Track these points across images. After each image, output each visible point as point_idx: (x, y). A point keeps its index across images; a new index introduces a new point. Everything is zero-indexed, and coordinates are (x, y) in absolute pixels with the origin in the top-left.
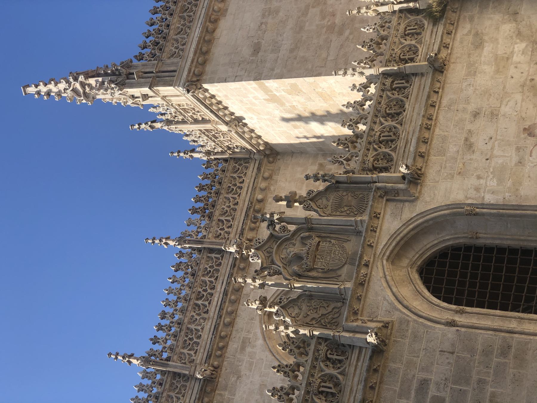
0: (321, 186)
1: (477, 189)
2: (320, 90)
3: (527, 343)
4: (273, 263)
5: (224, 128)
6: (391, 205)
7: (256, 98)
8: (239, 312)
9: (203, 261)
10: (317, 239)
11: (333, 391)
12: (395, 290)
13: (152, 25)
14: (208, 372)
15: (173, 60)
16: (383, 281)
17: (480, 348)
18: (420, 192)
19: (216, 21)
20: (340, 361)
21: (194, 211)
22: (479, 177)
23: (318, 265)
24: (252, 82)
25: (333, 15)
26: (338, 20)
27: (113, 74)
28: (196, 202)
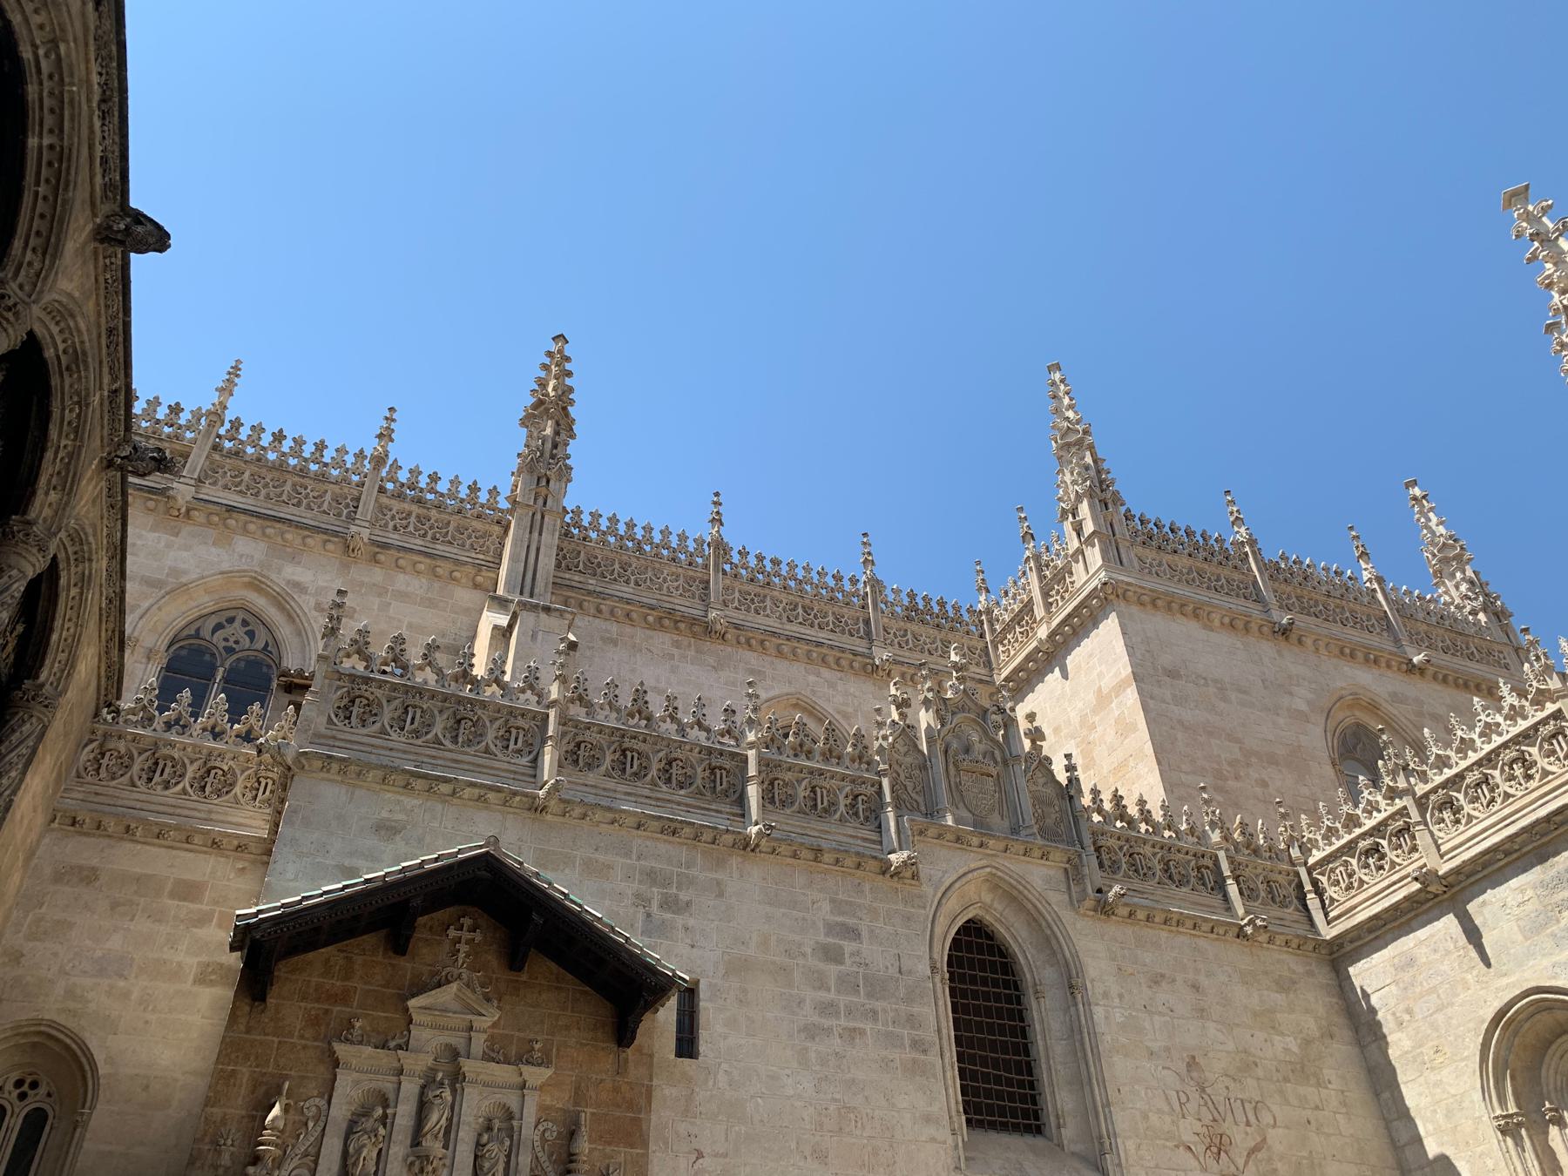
0: (1062, 777)
1: (1106, 995)
2: (1131, 764)
3: (934, 1076)
4: (953, 713)
5: (1043, 632)
6: (1061, 875)
7: (1101, 675)
8: (796, 664)
9: (852, 613)
10: (995, 773)
12: (957, 885)
13: (1172, 531)
14: (718, 627)
15: (1135, 560)
16: (965, 869)
17: (916, 1010)
18: (1085, 915)
19: (1196, 616)
20: (856, 814)
21: (912, 595)
22: (1121, 996)
23: (964, 778)
24: (1129, 670)
25: (1237, 778)
26: (1231, 784)
27: (1101, 482)
28: (924, 598)
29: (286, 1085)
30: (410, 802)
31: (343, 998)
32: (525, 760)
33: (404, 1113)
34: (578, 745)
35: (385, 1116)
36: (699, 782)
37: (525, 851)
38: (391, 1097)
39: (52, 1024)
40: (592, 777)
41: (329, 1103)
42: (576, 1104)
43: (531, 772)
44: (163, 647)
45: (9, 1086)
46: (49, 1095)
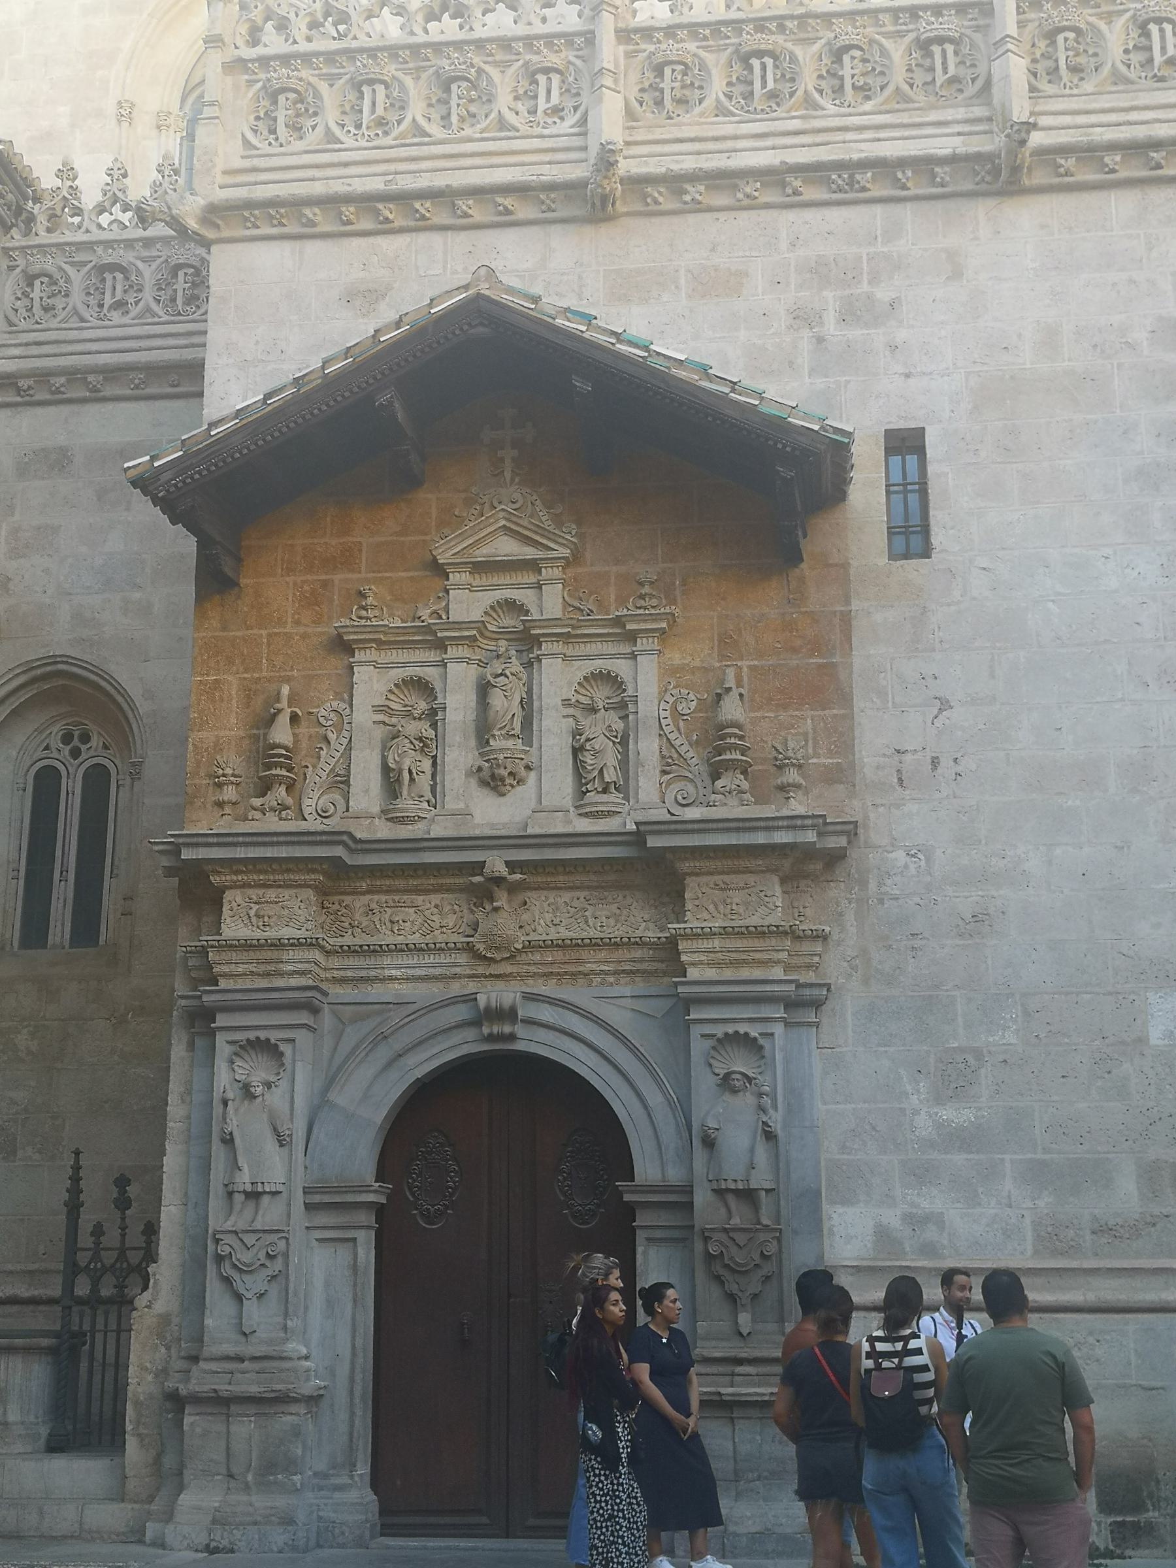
11: (1158, 59)
29: (286, 690)
30: (387, 244)
31: (347, 559)
32: (567, 125)
33: (459, 706)
34: (659, 70)
35: (433, 712)
36: (898, 77)
37: (564, 279)
38: (438, 686)
39: (66, 659)
40: (690, 124)
41: (351, 706)
42: (723, 657)
43: (577, 141)
44: (175, 109)
45: (56, 742)
46: (105, 747)
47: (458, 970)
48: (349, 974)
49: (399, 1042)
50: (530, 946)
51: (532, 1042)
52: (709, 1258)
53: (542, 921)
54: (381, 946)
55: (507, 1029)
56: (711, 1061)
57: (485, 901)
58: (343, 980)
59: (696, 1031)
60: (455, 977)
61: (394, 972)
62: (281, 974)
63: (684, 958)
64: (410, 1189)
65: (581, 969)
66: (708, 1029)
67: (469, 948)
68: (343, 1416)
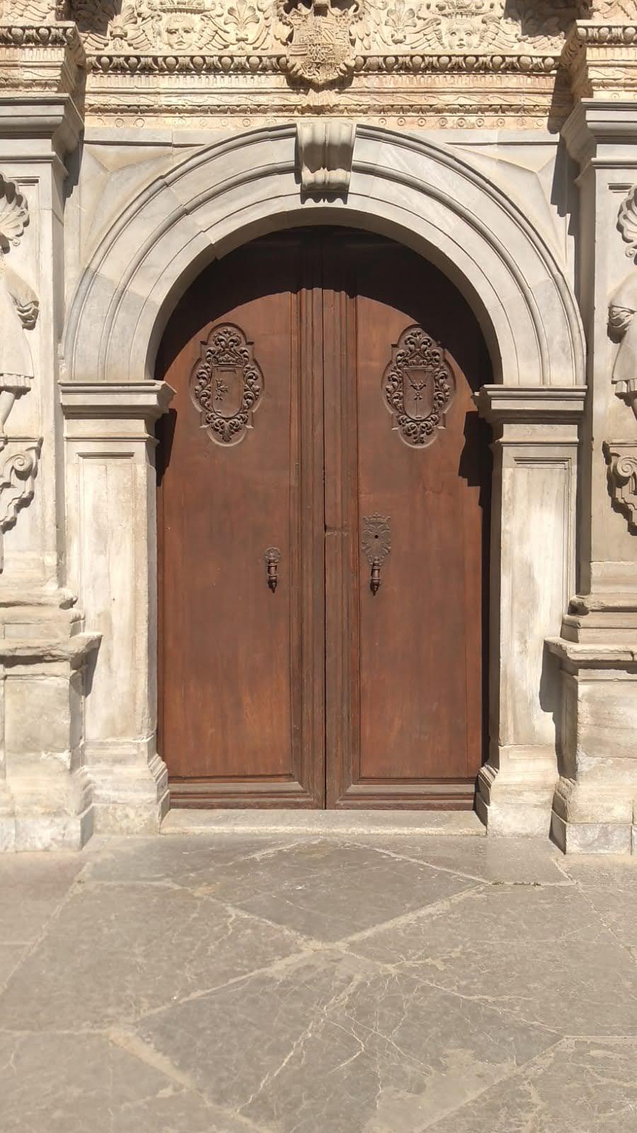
47: (262, 99)
48: (113, 101)
49: (184, 192)
50: (366, 67)
51: (368, 198)
52: (615, 481)
53: (377, 36)
54: (155, 59)
55: (338, 175)
56: (624, 222)
57: (300, 5)
58: (101, 110)
59: (604, 178)
60: (259, 110)
61: (174, 101)
62: (15, 86)
63: (593, 74)
64: (197, 397)
65: (432, 101)
66: (620, 176)
67: (279, 67)
68: (123, 673)
